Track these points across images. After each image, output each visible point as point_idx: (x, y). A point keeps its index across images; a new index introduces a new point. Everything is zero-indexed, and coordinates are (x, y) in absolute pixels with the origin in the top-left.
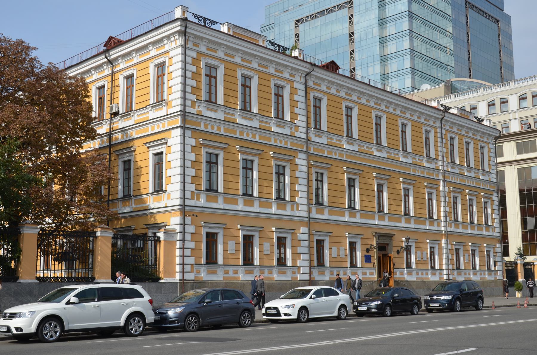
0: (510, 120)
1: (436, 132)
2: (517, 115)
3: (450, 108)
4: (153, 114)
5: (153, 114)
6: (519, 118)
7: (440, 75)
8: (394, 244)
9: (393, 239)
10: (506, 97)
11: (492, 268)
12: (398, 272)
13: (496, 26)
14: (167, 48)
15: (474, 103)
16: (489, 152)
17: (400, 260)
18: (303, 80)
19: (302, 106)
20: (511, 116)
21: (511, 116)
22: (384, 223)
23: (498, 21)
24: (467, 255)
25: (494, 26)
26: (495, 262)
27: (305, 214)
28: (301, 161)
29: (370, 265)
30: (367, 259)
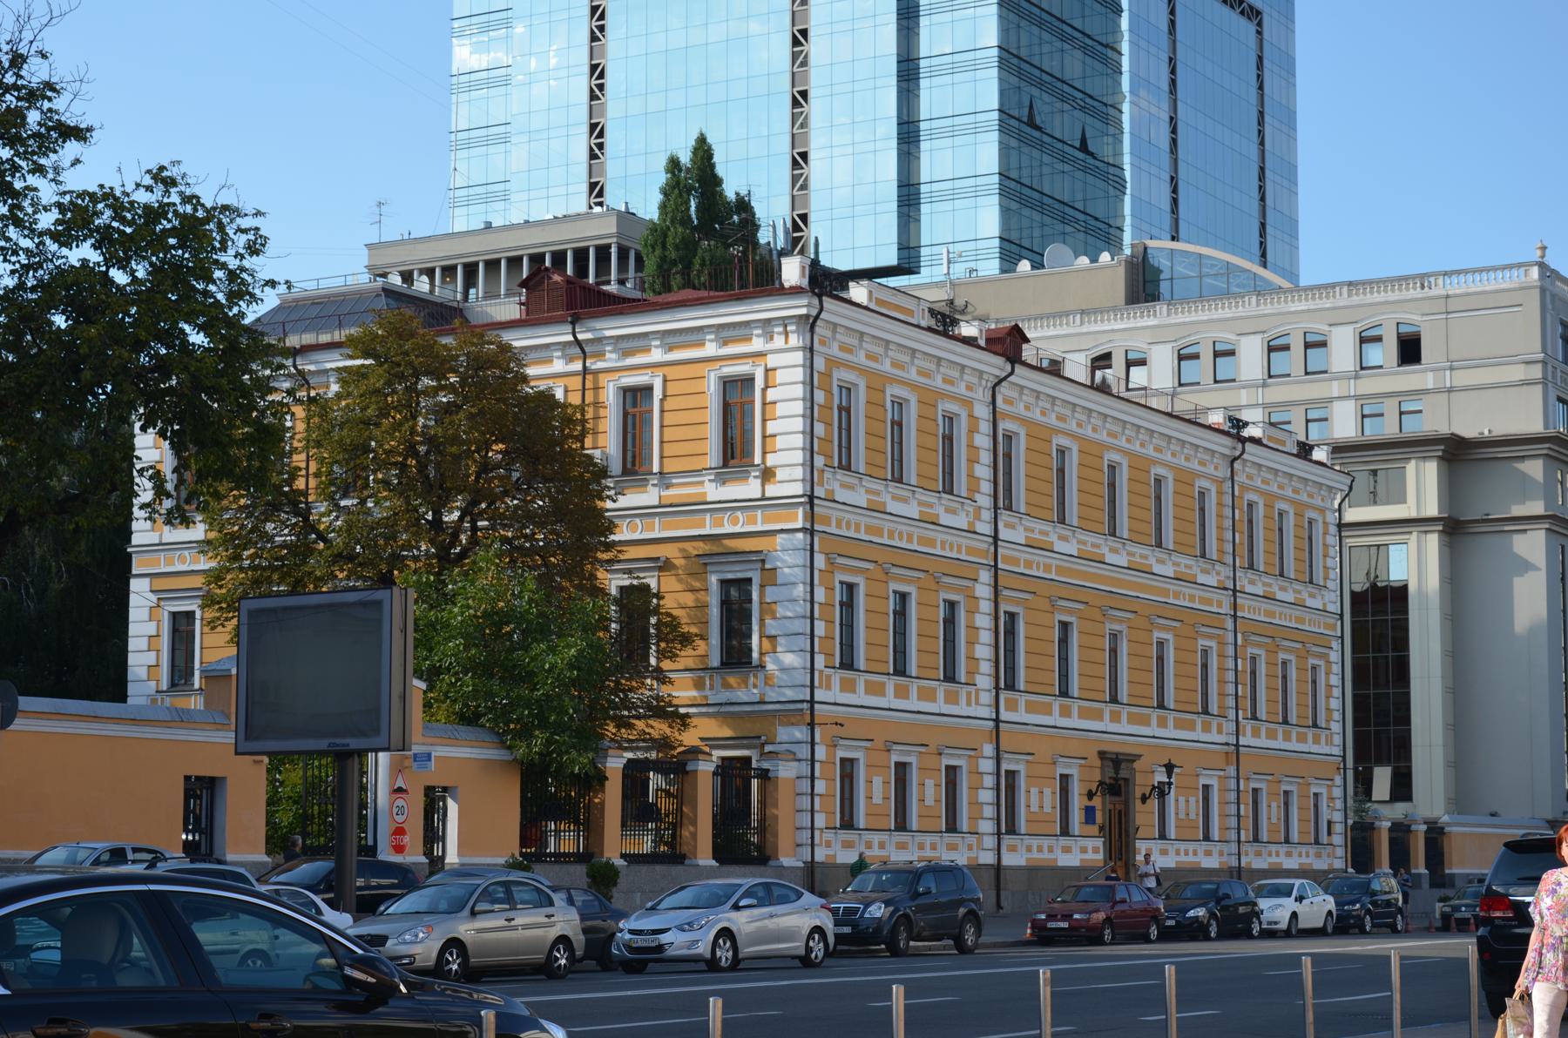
0: (1331, 400)
1: (1220, 493)
2: (1353, 387)
3: (1246, 424)
4: (714, 492)
5: (714, 492)
6: (1357, 398)
7: (1079, 196)
8: (1139, 778)
9: (1136, 765)
10: (1324, 328)
11: (1324, 838)
12: (1142, 846)
13: (1252, 28)
14: (757, 344)
15: (1226, 336)
16: (1325, 533)
17: (1145, 816)
18: (989, 394)
19: (986, 457)
20: (1335, 389)
21: (1335, 389)
22: (1119, 728)
23: (1259, 13)
24: (1274, 805)
25: (1247, 28)
26: (1330, 823)
27: (987, 712)
28: (983, 590)
29: (1094, 829)
30: (1089, 813)
